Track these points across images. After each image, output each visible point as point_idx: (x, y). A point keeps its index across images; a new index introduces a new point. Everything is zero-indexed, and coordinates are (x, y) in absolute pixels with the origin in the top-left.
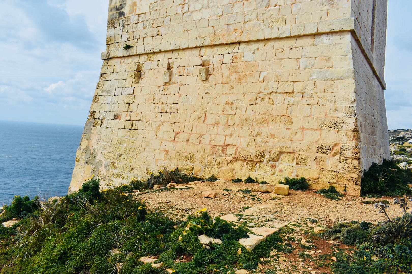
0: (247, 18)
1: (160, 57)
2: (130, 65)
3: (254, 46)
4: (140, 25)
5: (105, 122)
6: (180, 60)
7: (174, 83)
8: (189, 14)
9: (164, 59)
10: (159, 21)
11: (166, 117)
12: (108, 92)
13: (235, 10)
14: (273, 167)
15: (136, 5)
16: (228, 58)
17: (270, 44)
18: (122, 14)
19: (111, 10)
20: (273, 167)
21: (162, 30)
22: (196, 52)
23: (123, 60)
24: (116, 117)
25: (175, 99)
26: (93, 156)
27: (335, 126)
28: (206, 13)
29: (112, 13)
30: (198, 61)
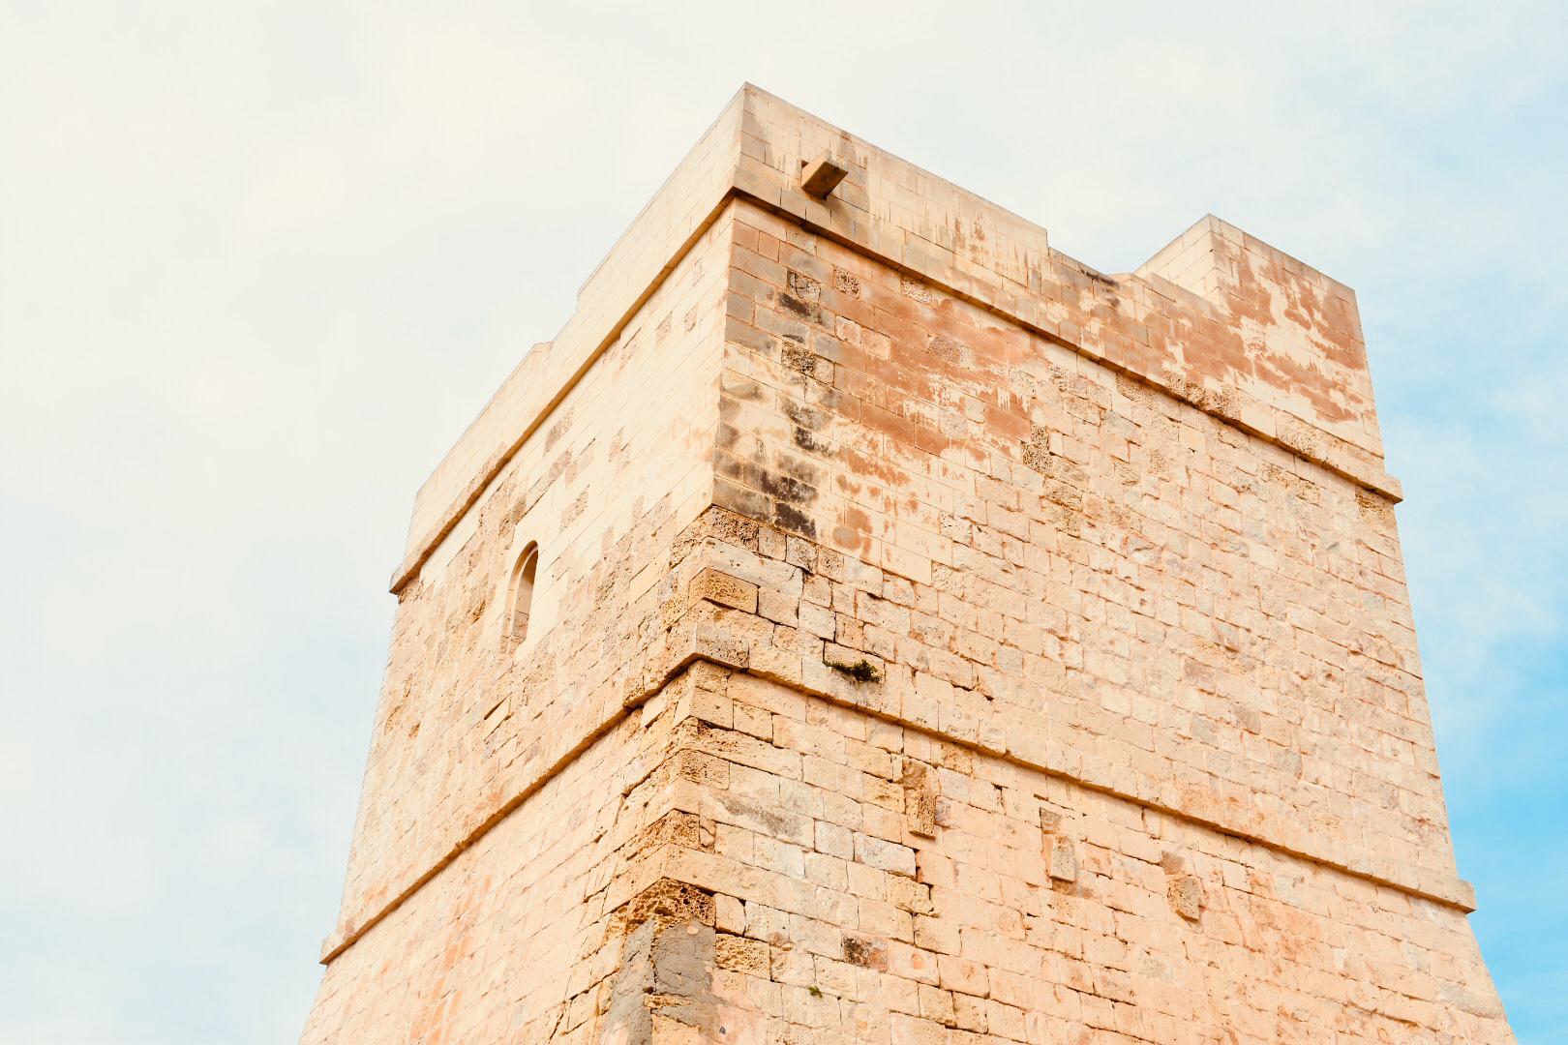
0: (1259, 782)
7: (1087, 894)
8: (1086, 678)
10: (982, 648)
11: (1109, 1016)
15: (868, 529)
17: (1327, 878)
19: (735, 470)
21: (993, 683)
23: (820, 711)
25: (1110, 952)
29: (739, 484)
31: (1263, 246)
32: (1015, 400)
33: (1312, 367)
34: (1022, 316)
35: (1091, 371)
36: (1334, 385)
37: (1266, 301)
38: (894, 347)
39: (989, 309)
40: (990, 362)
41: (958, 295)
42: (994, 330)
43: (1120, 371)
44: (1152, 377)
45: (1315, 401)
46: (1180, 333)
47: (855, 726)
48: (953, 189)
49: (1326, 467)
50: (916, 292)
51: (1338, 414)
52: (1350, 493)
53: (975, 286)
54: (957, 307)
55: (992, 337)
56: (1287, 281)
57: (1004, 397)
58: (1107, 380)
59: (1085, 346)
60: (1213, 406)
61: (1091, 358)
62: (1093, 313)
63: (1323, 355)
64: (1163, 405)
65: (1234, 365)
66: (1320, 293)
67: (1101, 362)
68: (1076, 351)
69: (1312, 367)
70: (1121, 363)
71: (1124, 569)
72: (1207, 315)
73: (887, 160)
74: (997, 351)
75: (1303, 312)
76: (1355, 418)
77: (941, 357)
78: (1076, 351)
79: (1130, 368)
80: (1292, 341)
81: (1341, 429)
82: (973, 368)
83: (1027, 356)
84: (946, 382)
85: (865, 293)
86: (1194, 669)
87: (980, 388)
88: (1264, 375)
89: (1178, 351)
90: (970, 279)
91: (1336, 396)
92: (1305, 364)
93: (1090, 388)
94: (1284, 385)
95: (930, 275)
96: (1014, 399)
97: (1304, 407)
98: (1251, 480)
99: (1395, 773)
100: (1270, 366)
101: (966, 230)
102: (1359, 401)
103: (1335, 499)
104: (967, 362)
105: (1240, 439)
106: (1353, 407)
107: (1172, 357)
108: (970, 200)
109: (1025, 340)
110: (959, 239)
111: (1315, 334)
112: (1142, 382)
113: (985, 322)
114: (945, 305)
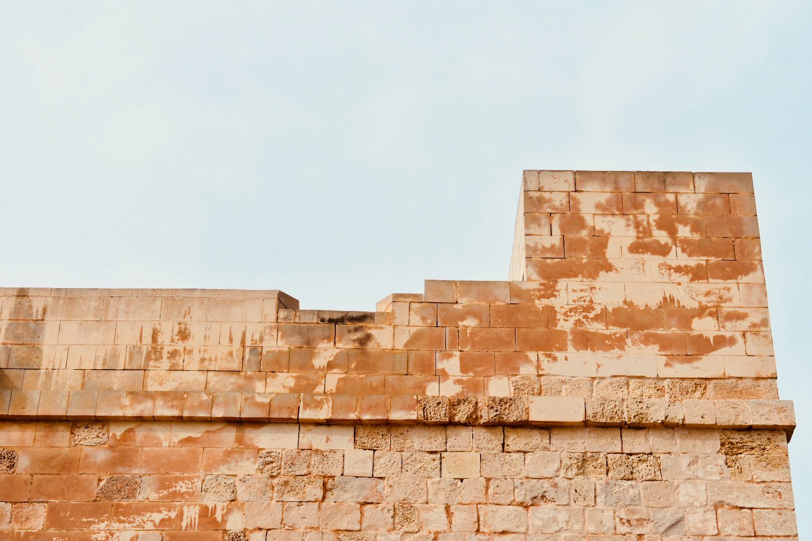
31: (603, 176)
32: (206, 514)
33: (668, 301)
34: (218, 413)
35: (316, 439)
36: (701, 312)
37: (600, 241)
38: (53, 512)
39: (180, 420)
40: (177, 479)
41: (140, 420)
42: (189, 440)
43: (356, 425)
44: (397, 415)
45: (665, 344)
46: (458, 338)
48: (155, 293)
49: (667, 426)
50: (87, 437)
51: (703, 346)
52: (711, 445)
53: (160, 402)
54: (141, 433)
55: (184, 450)
56: (638, 206)
57: (191, 513)
58: (342, 440)
59: (305, 415)
60: (486, 415)
61: (318, 424)
62: (330, 366)
63: (685, 279)
64: (419, 441)
65: (536, 348)
66: (690, 201)
67: (329, 423)
68: (299, 423)
69: (668, 301)
70: (352, 416)
72: (504, 298)
73: (69, 298)
74: (187, 465)
75: (662, 236)
76: (732, 341)
77: (115, 501)
78: (299, 423)
79: (366, 417)
80: (636, 280)
81: (708, 365)
82: (153, 496)
83: (229, 453)
84: (116, 525)
85: (23, 463)
87: (157, 517)
88: (585, 341)
89: (452, 365)
90: (151, 396)
91: (705, 327)
92: (654, 301)
93: (315, 459)
94: (619, 342)
95: (101, 413)
96: (206, 514)
97: (643, 359)
98: (546, 485)
101: (164, 339)
102: (741, 317)
103: (685, 461)
104: (148, 493)
105: (536, 439)
106: (730, 329)
107: (442, 375)
108: (173, 299)
109: (229, 435)
110: (155, 352)
111: (678, 258)
112: (389, 425)
113: (182, 433)
114: (124, 438)
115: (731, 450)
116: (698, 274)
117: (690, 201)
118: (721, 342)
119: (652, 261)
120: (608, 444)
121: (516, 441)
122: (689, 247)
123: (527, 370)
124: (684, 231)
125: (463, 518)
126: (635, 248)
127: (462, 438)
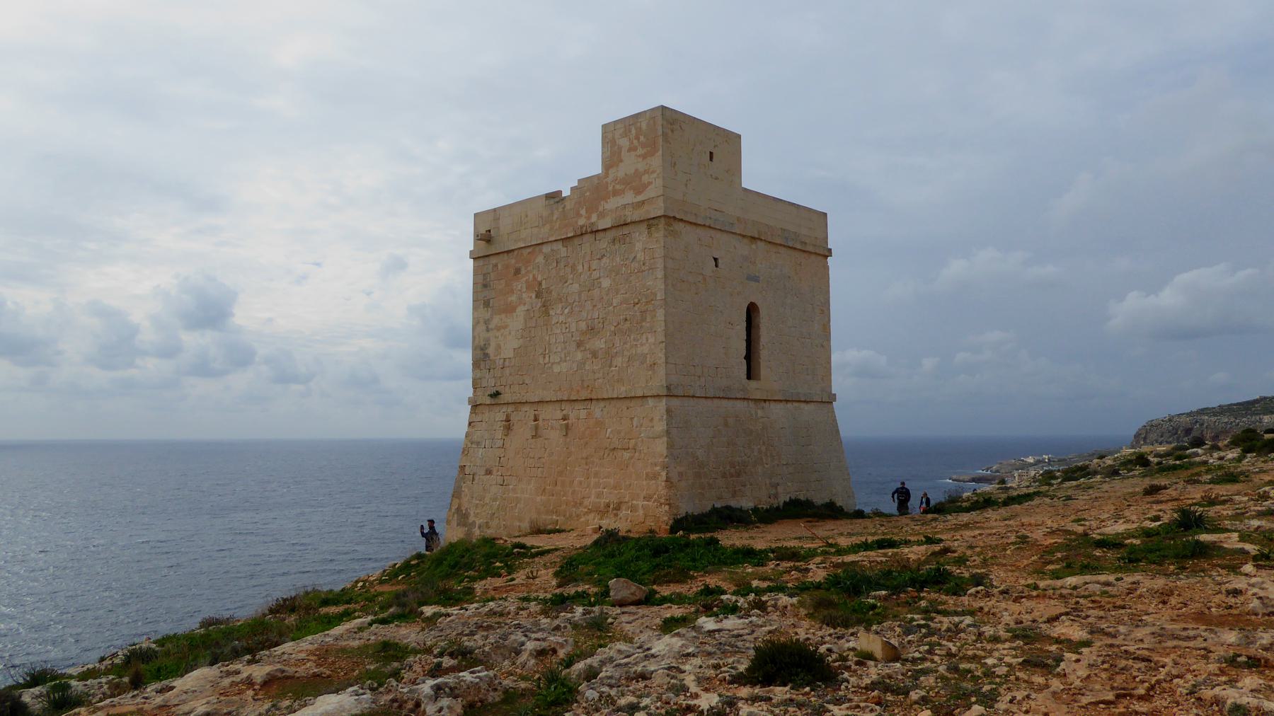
0: (597, 376)
1: (526, 408)
2: (499, 415)
3: (602, 404)
4: (507, 371)
5: (477, 478)
6: (548, 413)
9: (529, 411)
12: (478, 443)
13: (587, 367)
14: (616, 515)
16: (583, 414)
17: (613, 402)
18: (486, 355)
20: (616, 515)
22: (557, 405)
24: (489, 472)
26: (466, 516)
27: (655, 477)
28: (564, 367)
30: (559, 415)
36: (646, 172)
47: (496, 409)
58: (559, 245)
64: (576, 241)
71: (562, 318)
86: (579, 344)
88: (616, 193)
99: (645, 349)
100: (618, 187)
111: (640, 151)
115: (649, 227)
116: (644, 157)
117: (644, 126)
118: (650, 183)
119: (633, 153)
120: (619, 233)
121: (599, 236)
122: (643, 145)
123: (601, 209)
124: (642, 138)
125: (586, 266)
126: (630, 150)
127: (586, 237)
